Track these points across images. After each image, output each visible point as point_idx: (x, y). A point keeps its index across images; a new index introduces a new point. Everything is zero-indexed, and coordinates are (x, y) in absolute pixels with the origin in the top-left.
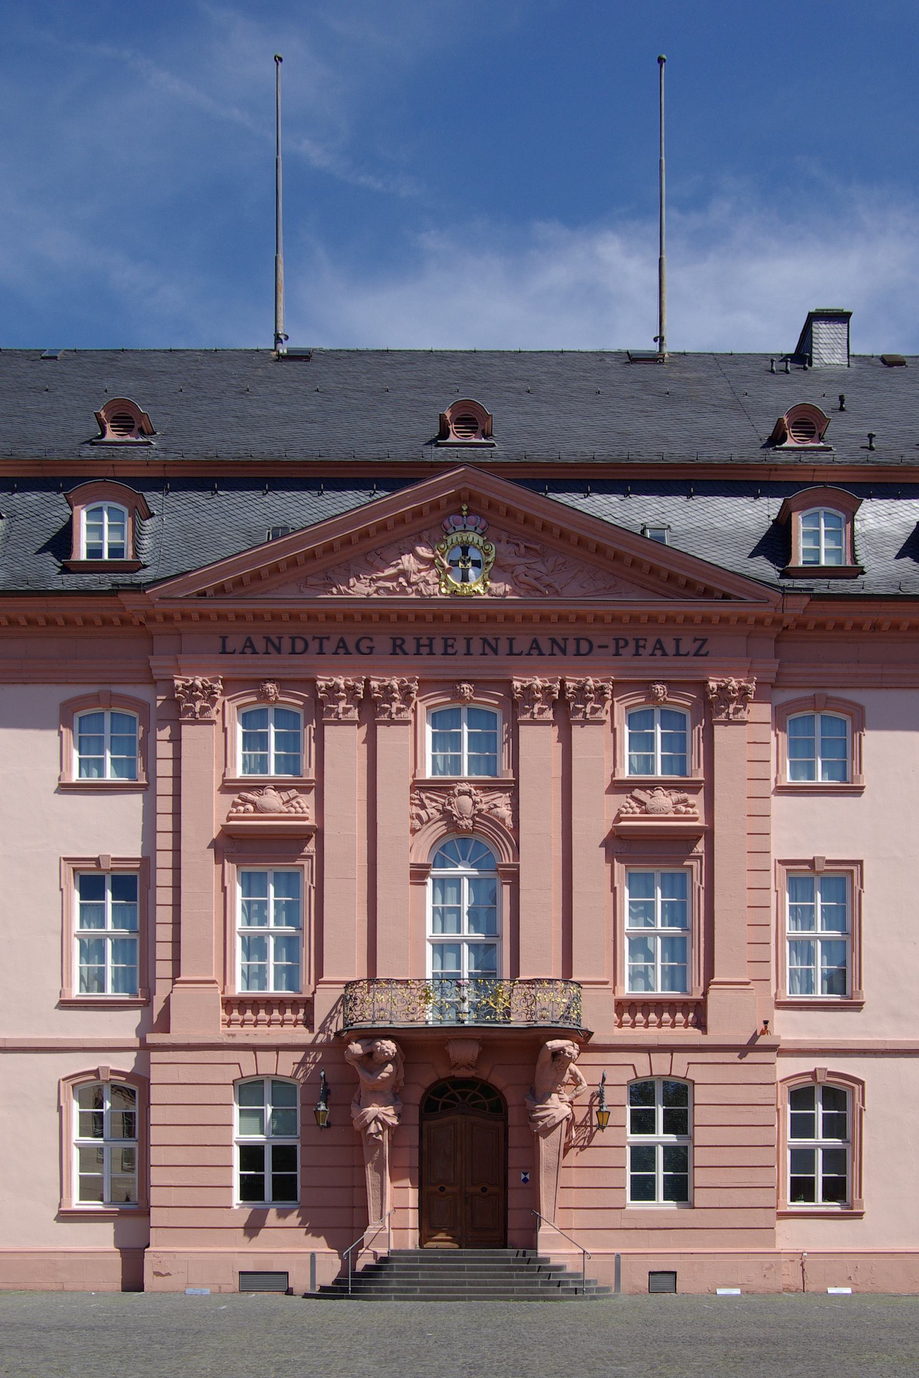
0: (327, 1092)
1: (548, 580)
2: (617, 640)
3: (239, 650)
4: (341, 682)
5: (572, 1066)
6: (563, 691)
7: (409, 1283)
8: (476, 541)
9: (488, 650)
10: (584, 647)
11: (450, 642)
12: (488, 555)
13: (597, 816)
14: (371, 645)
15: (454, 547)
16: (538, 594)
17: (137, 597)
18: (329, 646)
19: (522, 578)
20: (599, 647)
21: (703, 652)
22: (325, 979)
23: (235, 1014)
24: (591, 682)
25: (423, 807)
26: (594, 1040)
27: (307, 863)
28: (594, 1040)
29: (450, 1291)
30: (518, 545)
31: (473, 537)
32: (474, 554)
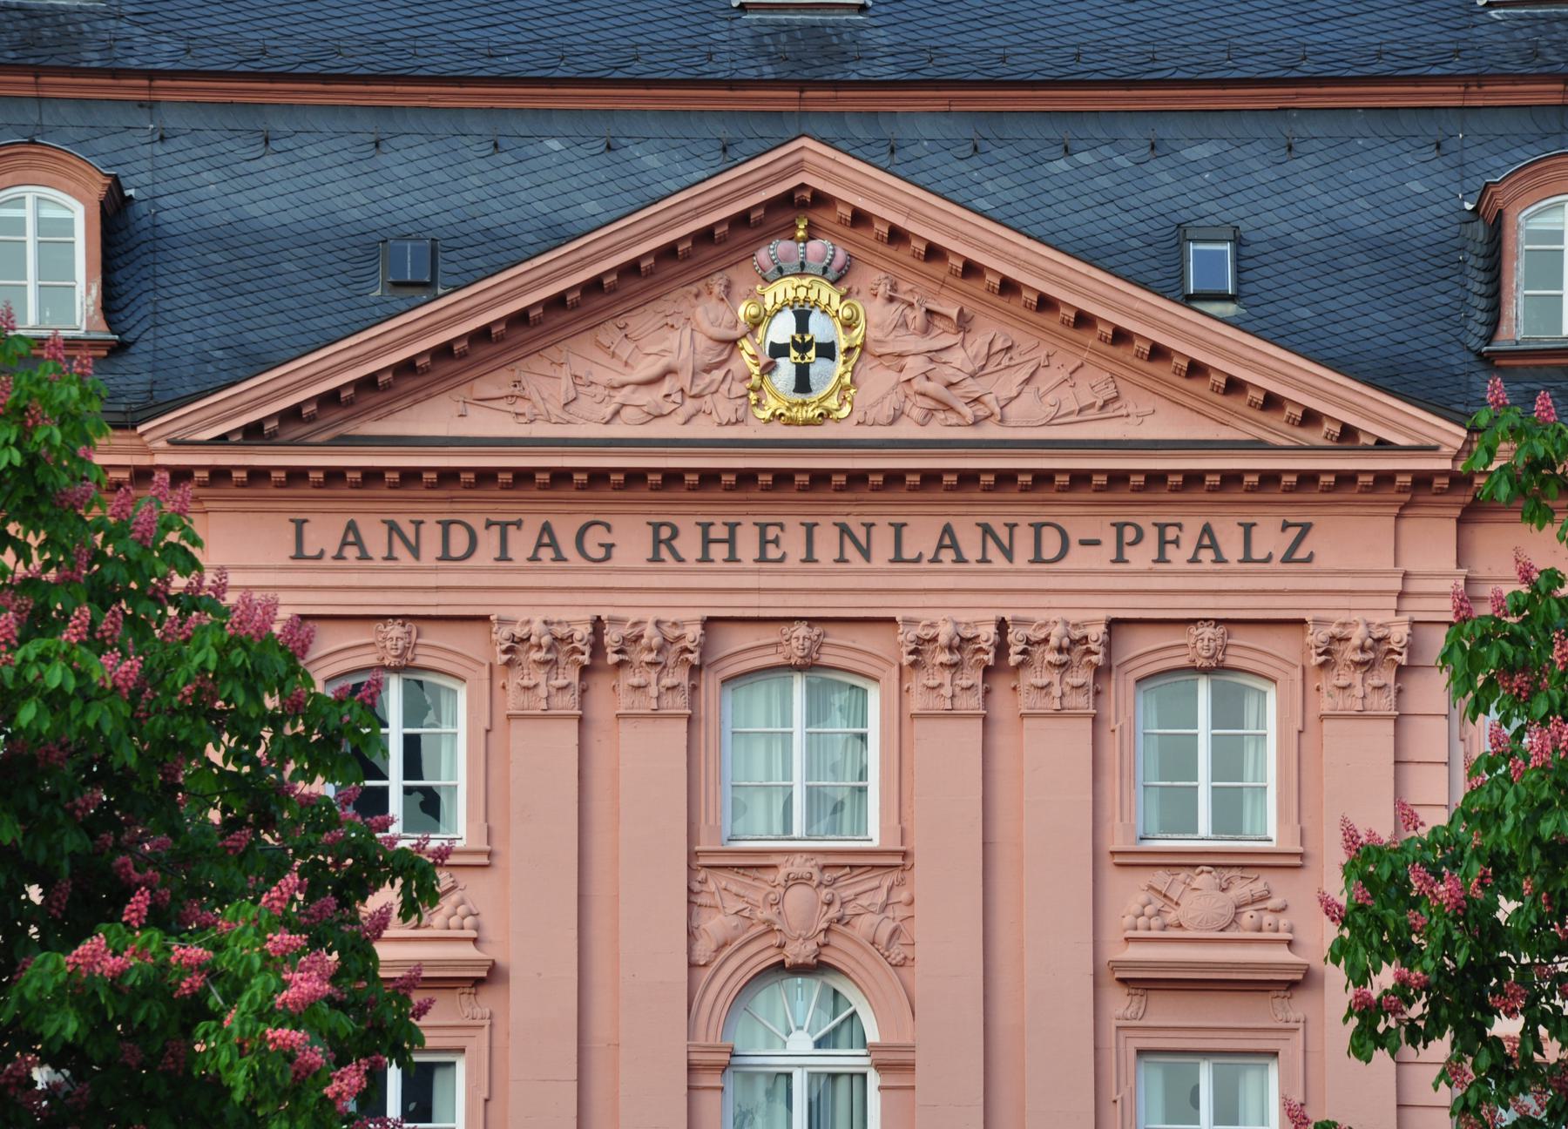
1: (974, 387)
2: (1119, 528)
3: (332, 550)
8: (824, 300)
11: (772, 533)
12: (848, 326)
14: (608, 540)
15: (779, 311)
16: (953, 418)
19: (921, 384)
20: (1084, 543)
21: (1301, 553)
30: (911, 305)
32: (820, 329)
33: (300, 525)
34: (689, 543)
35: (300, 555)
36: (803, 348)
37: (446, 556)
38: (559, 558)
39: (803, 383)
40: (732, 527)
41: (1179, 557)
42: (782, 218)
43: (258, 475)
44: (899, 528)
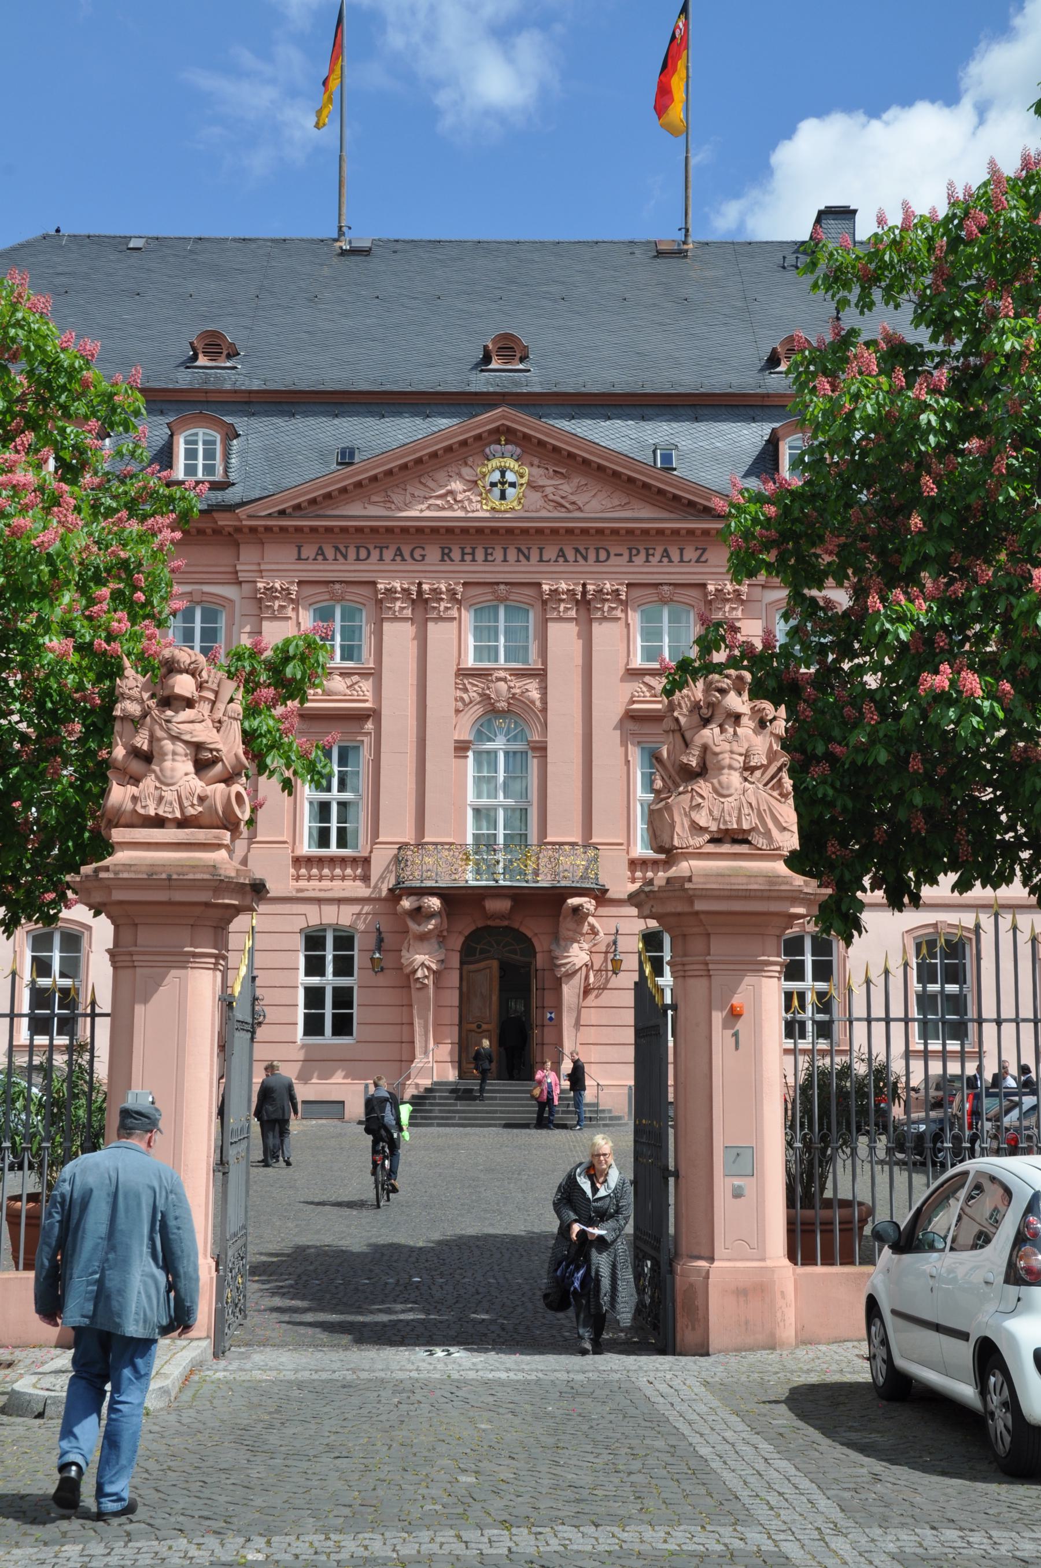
0: (380, 940)
1: (573, 498)
2: (630, 549)
3: (312, 556)
4: (397, 585)
5: (591, 919)
6: (584, 593)
7: (449, 1112)
9: (521, 558)
10: (603, 555)
11: (490, 551)
12: (522, 477)
13: (613, 699)
17: (228, 515)
18: (388, 554)
19: (551, 497)
21: (703, 559)
22: (380, 840)
23: (303, 871)
24: (608, 586)
25: (466, 690)
26: (609, 895)
27: (366, 739)
28: (609, 895)
29: (484, 1119)
31: (511, 463)
32: (510, 477)
33: (299, 548)
34: (456, 554)
35: (299, 559)
36: (503, 483)
37: (358, 559)
38: (403, 560)
39: (503, 496)
40: (474, 549)
41: (654, 560)
42: (494, 438)
43: (283, 529)
44: (541, 550)
